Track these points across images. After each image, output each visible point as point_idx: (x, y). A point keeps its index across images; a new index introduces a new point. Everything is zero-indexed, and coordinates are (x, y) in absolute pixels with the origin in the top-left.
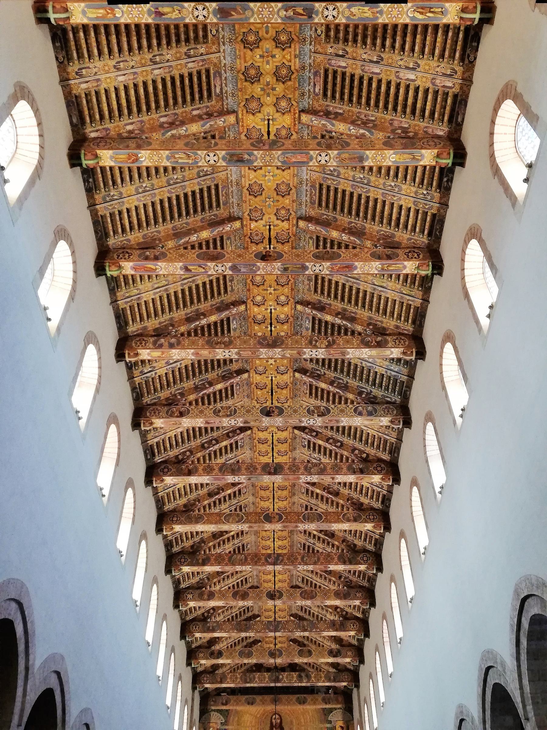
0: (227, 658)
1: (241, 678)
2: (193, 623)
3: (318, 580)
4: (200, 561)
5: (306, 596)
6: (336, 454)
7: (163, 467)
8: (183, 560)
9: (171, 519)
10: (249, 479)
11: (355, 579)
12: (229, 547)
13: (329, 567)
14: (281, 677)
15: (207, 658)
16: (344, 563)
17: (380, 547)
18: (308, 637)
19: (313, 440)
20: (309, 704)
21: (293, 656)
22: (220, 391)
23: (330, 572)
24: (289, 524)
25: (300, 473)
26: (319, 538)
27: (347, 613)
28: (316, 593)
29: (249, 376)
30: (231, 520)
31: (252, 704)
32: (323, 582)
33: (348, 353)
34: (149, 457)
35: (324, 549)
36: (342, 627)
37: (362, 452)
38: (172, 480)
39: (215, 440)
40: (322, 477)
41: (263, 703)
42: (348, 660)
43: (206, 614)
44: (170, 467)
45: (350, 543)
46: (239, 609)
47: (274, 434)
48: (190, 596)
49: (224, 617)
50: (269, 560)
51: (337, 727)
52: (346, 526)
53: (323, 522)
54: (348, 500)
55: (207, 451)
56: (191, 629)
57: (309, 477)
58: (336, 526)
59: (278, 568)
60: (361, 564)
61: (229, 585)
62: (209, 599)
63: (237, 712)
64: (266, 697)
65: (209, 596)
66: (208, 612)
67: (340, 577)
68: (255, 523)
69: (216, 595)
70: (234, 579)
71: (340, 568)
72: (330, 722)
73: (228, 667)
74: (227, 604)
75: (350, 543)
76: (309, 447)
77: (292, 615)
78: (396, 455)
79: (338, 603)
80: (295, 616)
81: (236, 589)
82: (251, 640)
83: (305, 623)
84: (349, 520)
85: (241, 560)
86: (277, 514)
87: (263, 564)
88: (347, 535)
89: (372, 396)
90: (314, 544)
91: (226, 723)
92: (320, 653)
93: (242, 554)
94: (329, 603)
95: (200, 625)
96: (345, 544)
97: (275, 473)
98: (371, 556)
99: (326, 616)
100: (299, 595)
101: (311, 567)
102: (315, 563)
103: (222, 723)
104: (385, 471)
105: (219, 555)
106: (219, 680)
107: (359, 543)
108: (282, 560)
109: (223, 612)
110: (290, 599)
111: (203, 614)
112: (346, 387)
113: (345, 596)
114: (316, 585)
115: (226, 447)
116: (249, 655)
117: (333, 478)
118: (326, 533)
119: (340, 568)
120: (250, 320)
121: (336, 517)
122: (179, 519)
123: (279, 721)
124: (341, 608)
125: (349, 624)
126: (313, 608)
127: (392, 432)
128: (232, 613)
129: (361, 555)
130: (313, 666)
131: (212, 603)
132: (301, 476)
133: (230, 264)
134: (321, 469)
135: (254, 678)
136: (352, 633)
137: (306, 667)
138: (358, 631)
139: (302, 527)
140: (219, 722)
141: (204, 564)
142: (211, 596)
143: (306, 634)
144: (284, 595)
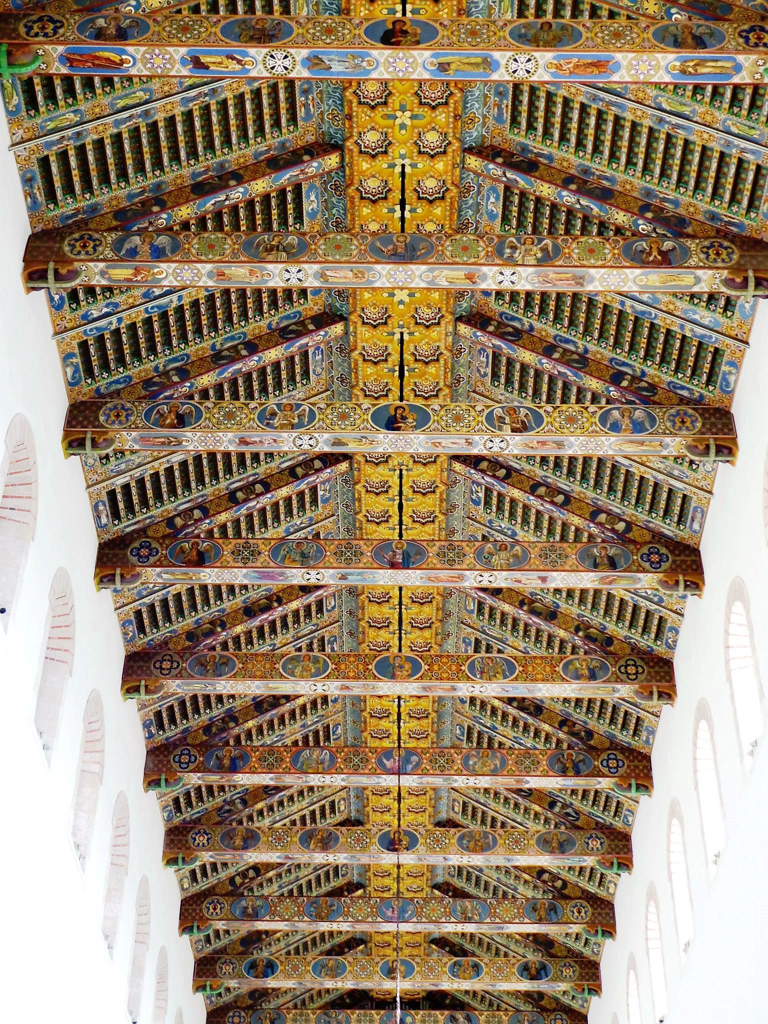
0: (288, 976)
2: (209, 900)
3: (502, 810)
4: (226, 762)
5: (472, 843)
7: (136, 544)
8: (185, 759)
9: (158, 665)
10: (343, 577)
11: (586, 808)
12: (293, 732)
13: (527, 782)
15: (240, 976)
16: (564, 773)
17: (648, 738)
18: (472, 935)
19: (498, 487)
21: (438, 977)
22: (276, 365)
23: (529, 794)
24: (437, 683)
25: (465, 566)
26: (505, 715)
27: (565, 883)
28: (494, 837)
29: (346, 333)
30: (298, 671)
32: (512, 814)
33: (592, 280)
34: (104, 520)
35: (516, 740)
36: (550, 914)
37: (615, 517)
38: (159, 575)
39: (262, 482)
40: (518, 575)
42: (563, 986)
43: (238, 880)
44: (155, 545)
45: (577, 727)
46: (316, 870)
47: (404, 472)
48: (202, 839)
49: (280, 887)
50: (388, 764)
52: (571, 690)
53: (516, 679)
54: (577, 629)
55: (244, 511)
56: (205, 911)
57: (486, 575)
58: (548, 690)
59: (409, 781)
60: (604, 776)
61: (296, 817)
62: (245, 848)
65: (245, 840)
66: (244, 875)
67: (552, 805)
68: (356, 678)
69: (263, 839)
70: (305, 803)
71: (552, 783)
73: (288, 997)
74: (287, 858)
75: (577, 727)
76: (487, 503)
77: (436, 886)
78: (696, 526)
79: (544, 860)
80: (445, 888)
81: (308, 827)
82: (343, 938)
83: (467, 903)
84: (578, 677)
85: (322, 763)
86: (408, 659)
87: (374, 773)
88: (571, 710)
89: (644, 384)
90: (494, 729)
92: (499, 970)
93: (323, 748)
94: (523, 860)
95: (226, 903)
96: (565, 729)
97: (406, 564)
98: (627, 758)
99: (515, 889)
100: (454, 841)
101: (484, 782)
102: (494, 773)
104: (668, 564)
105: (271, 749)
107: (601, 727)
108: (418, 764)
109: (279, 876)
110: (432, 850)
111: (232, 880)
112: (582, 362)
113: (562, 848)
114: (494, 819)
115: (288, 500)
116: (336, 972)
117: (544, 580)
118: (522, 704)
119: (552, 783)
120: (351, 191)
121: (548, 669)
122: (175, 665)
124: (550, 873)
125: (567, 909)
126: (486, 871)
127: (689, 473)
128: (297, 879)
129: (604, 756)
130: (483, 997)
131: (253, 857)
132: (467, 573)
133: (305, 53)
134: (515, 556)
136: (575, 929)
137: (467, 999)
138: (592, 924)
139: (465, 689)
141: (234, 768)
142: (250, 840)
143: (470, 928)
144: (421, 841)
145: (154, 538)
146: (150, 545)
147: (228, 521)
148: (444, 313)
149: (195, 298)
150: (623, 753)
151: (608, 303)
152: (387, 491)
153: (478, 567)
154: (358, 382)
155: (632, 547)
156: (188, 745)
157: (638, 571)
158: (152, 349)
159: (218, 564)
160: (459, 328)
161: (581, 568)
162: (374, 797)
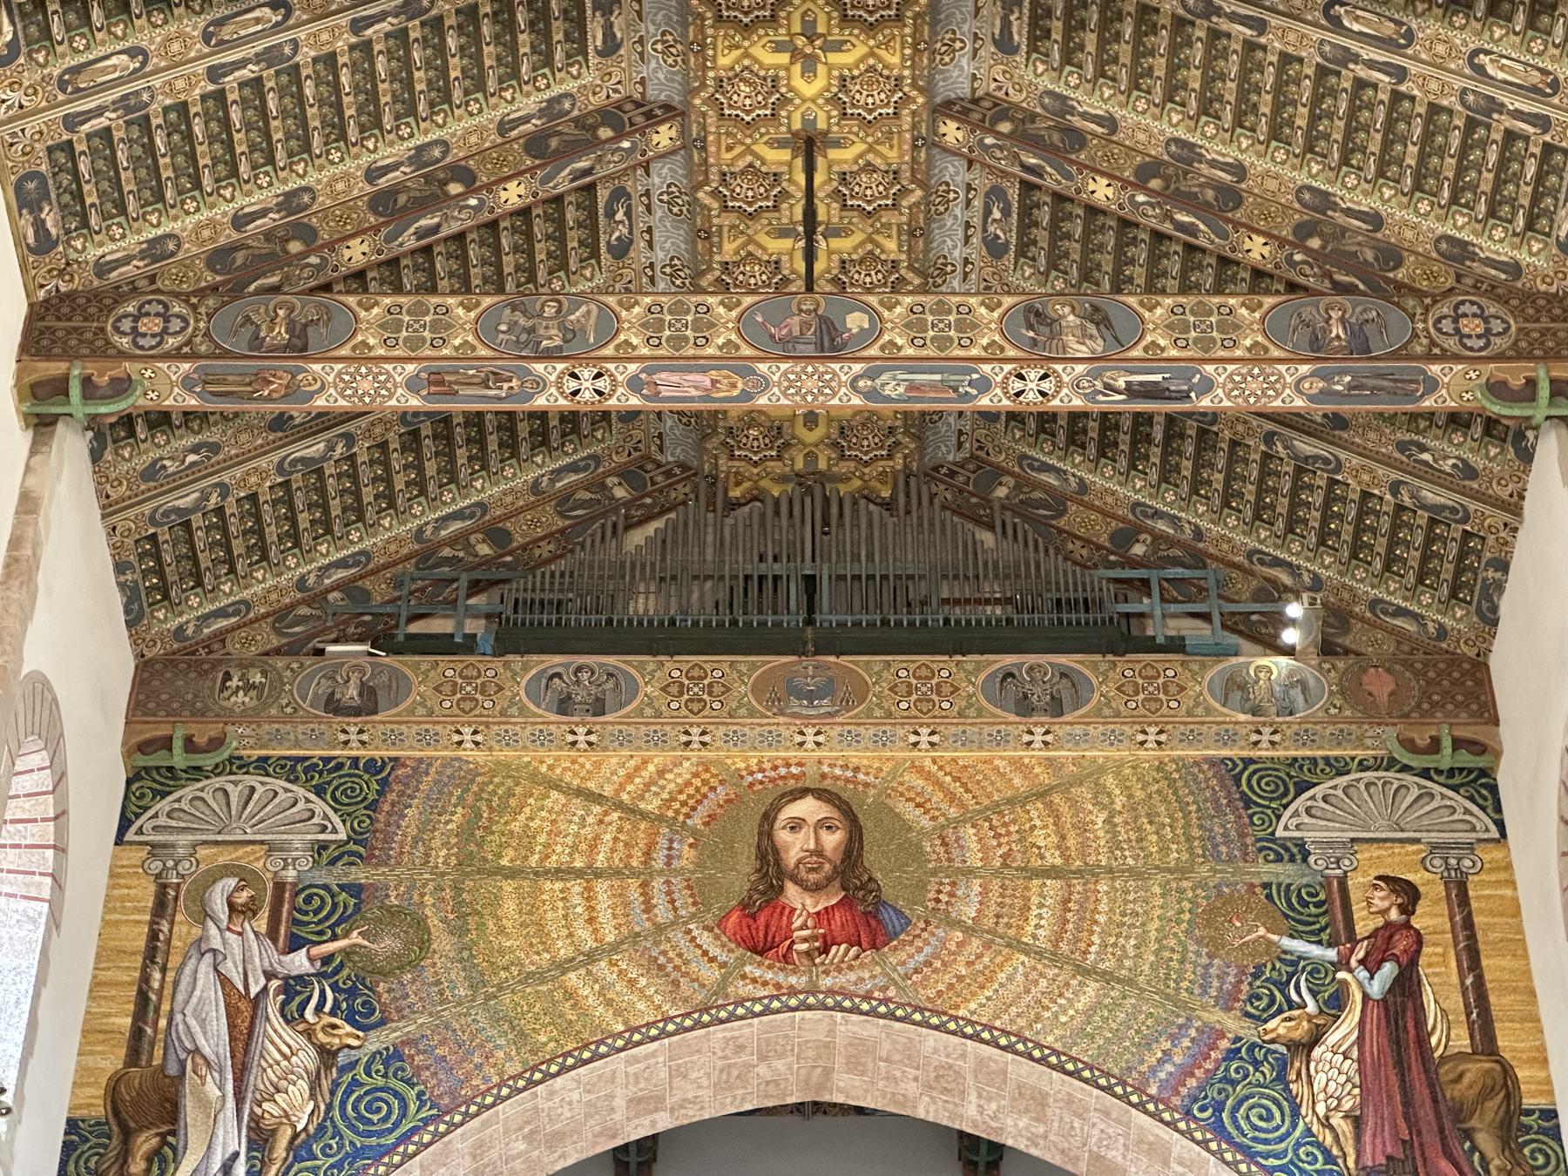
1: (485, 327)
14: (856, 321)
31: (599, 708)
41: (696, 705)
51: (1356, 882)
63: (466, 776)
64: (717, 666)
72: (1298, 852)
91: (362, 847)
103: (323, 846)
106: (281, 333)
123: (832, 841)
135: (609, 326)
140: (300, 840)
145: (177, 295)
146: (166, 306)
149: (326, 49)
150: (1503, 300)
151: (1290, 50)
152: (776, 208)
153: (1011, 352)
155: (1411, 303)
156: (158, 291)
157: (1430, 358)
161: (1276, 353)
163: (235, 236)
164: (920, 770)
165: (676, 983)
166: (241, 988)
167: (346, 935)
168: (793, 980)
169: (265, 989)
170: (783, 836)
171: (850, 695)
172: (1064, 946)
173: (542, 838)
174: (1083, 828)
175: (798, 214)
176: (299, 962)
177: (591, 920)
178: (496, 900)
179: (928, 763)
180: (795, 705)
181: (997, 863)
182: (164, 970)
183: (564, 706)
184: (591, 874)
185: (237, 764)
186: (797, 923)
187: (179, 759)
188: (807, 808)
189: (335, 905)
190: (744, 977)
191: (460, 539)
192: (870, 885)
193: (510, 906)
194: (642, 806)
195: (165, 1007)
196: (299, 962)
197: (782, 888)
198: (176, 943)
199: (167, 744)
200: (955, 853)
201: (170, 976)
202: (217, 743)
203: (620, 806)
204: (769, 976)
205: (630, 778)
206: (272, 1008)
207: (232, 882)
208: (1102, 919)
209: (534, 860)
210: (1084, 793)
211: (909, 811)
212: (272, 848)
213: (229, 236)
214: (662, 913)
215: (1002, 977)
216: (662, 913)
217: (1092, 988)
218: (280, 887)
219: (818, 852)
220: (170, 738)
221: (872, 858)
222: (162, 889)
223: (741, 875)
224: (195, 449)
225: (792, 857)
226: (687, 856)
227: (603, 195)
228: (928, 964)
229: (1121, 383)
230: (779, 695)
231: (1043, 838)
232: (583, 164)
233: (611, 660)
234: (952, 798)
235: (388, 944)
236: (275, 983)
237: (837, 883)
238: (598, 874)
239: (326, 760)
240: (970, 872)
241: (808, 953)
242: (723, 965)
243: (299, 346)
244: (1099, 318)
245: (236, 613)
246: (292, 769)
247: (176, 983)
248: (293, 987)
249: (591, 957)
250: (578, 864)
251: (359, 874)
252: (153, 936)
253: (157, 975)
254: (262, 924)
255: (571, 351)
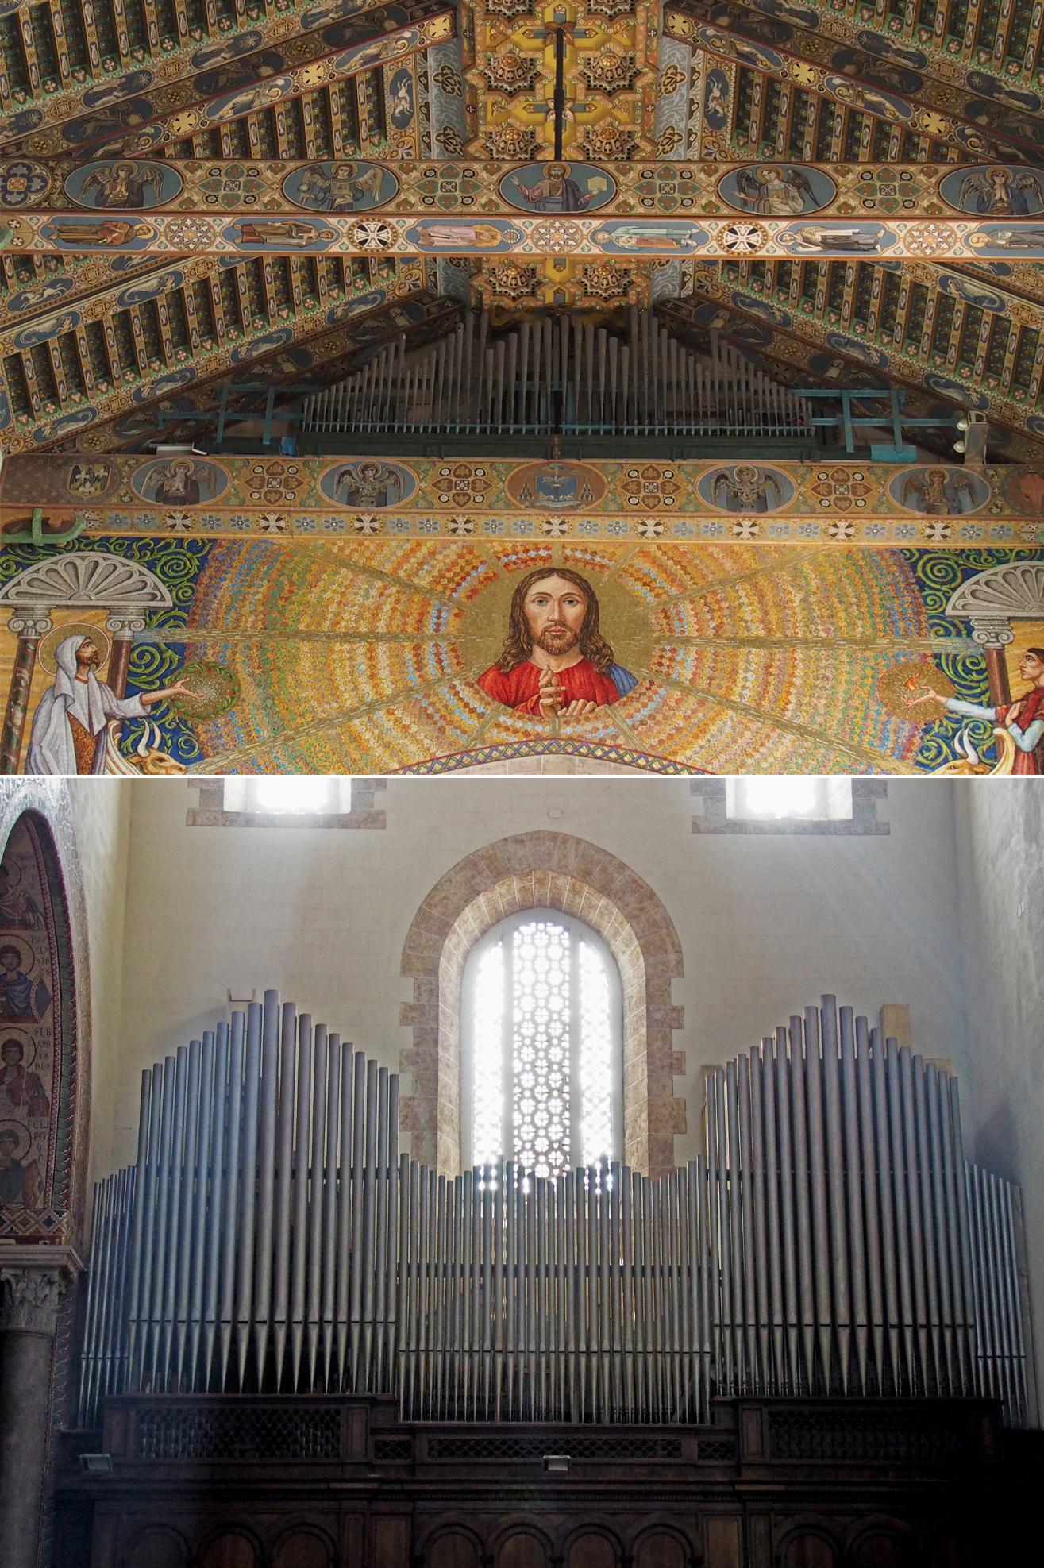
1: (288, 187)
6: (860, 312)
19: (763, 63)
20: (795, 512)
31: (381, 500)
41: (461, 500)
55: (227, 112)
57: (743, 229)
63: (270, 556)
76: (740, 125)
91: (186, 612)
103: (153, 612)
106: (122, 190)
123: (573, 612)
135: (392, 185)
140: (134, 605)
145: (38, 160)
146: (29, 169)
147: (195, 133)
148: (639, 67)
152: (531, 88)
153: (725, 211)
154: (473, 59)
156: (24, 156)
158: (82, 59)
159: (173, 207)
160: (671, 22)
162: (490, 99)
163: (86, 110)
164: (646, 554)
165: (441, 730)
166: (86, 726)
167: (172, 685)
168: (539, 728)
169: (106, 728)
170: (532, 608)
171: (589, 494)
172: (766, 705)
173: (333, 608)
174: (781, 605)
175: (550, 93)
176: (133, 707)
177: (372, 676)
178: (296, 657)
179: (654, 548)
180: (543, 499)
181: (711, 633)
182: (25, 710)
183: (353, 498)
184: (372, 638)
185: (84, 543)
186: (543, 681)
187: (38, 537)
188: (553, 585)
189: (163, 660)
190: (498, 725)
191: (268, 358)
192: (604, 651)
193: (306, 664)
194: (416, 581)
195: (26, 741)
196: (133, 707)
197: (531, 652)
198: (34, 688)
199: (26, 526)
200: (676, 623)
201: (30, 715)
202: (68, 526)
203: (397, 581)
204: (519, 725)
205: (406, 558)
206: (111, 742)
207: (80, 640)
208: (797, 681)
209: (326, 626)
210: (785, 576)
211: (639, 589)
212: (111, 612)
213: (81, 110)
214: (432, 670)
215: (713, 729)
216: (432, 670)
217: (789, 738)
218: (118, 645)
219: (562, 622)
220: (31, 520)
221: (607, 627)
222: (25, 642)
223: (495, 642)
224: (52, 285)
225: (539, 626)
226: (451, 623)
227: (389, 75)
228: (651, 717)
229: (818, 237)
230: (527, 493)
231: (749, 613)
232: (372, 50)
233: (392, 461)
234: (672, 579)
235: (206, 693)
236: (114, 724)
237: (577, 648)
238: (380, 638)
239: (157, 540)
240: (687, 641)
241: (552, 707)
242: (482, 715)
243: (136, 202)
244: (800, 182)
245: (85, 418)
246: (128, 547)
247: (34, 721)
248: (128, 727)
249: (372, 707)
250: (363, 629)
251: (183, 635)
252: (16, 682)
253: (19, 714)
254: (103, 674)
255: (360, 206)
